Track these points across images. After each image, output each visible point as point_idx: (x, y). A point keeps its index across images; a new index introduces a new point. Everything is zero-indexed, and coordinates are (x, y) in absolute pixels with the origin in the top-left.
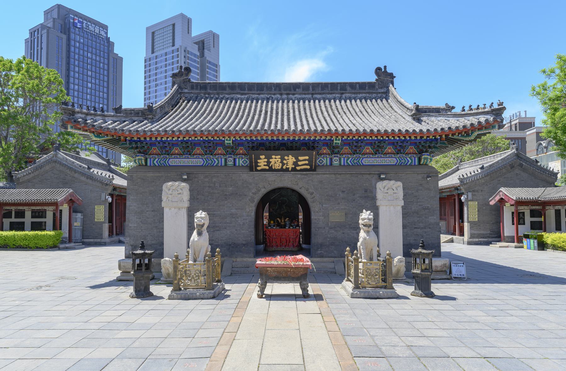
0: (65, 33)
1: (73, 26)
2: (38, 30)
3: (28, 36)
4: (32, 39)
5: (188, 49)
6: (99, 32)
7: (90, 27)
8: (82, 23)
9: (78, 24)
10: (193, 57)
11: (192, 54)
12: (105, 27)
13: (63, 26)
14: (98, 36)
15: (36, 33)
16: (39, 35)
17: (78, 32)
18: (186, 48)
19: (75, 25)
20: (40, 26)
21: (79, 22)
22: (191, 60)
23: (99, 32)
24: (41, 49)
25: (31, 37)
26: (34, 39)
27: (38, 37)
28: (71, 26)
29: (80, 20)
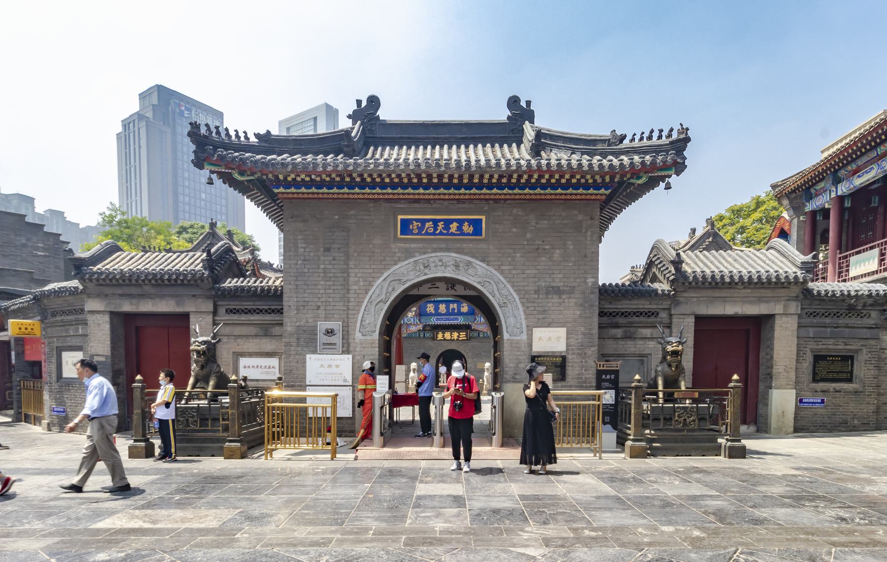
4: (127, 133)
7: (200, 115)
9: (186, 112)
15: (131, 125)
16: (136, 129)
20: (136, 117)
21: (187, 109)
24: (140, 147)
25: (125, 131)
26: (129, 134)
27: (134, 131)
29: (187, 106)
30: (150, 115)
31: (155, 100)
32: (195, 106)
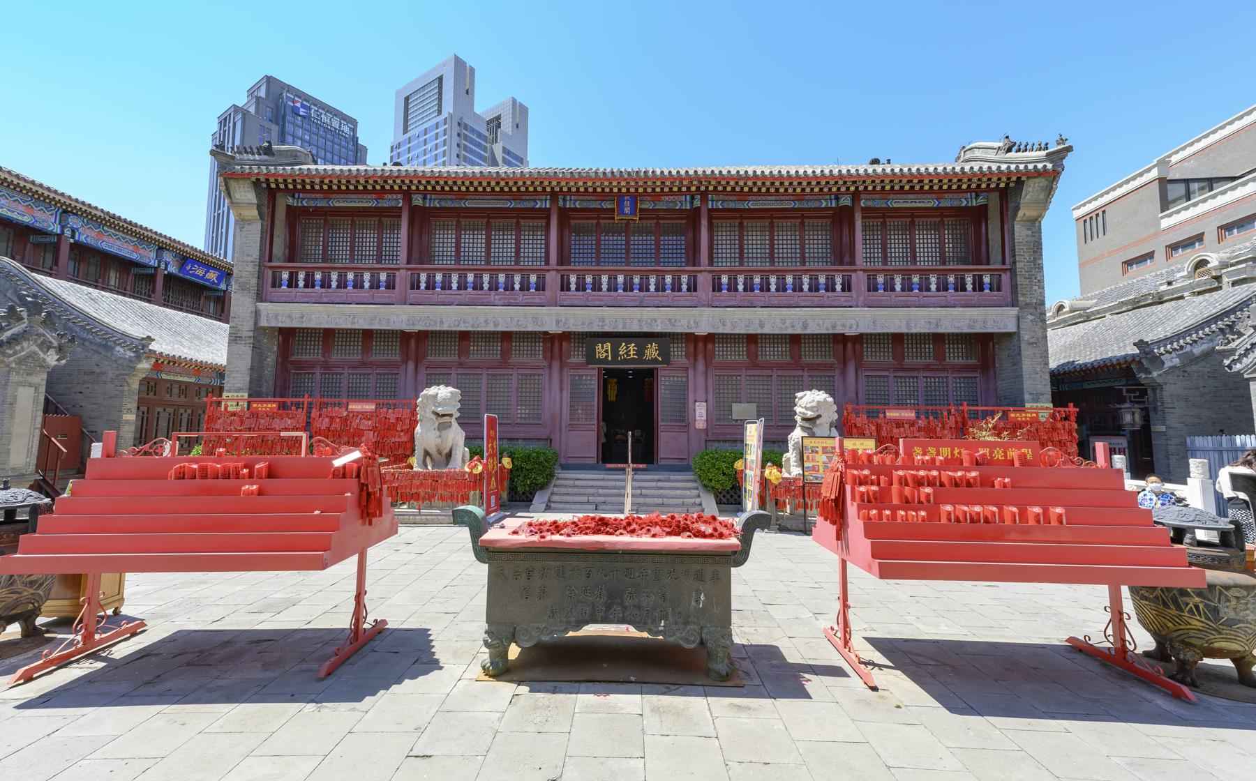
0: (277, 123)
1: (293, 112)
2: (230, 115)
3: (215, 128)
4: (222, 132)
5: (465, 120)
6: (340, 127)
8: (310, 109)
9: (301, 110)
10: (475, 137)
11: (473, 131)
12: (353, 123)
13: (275, 112)
14: (337, 133)
16: (231, 125)
17: (300, 123)
18: (461, 119)
19: (295, 112)
22: (471, 143)
23: (340, 127)
28: (289, 112)
29: (305, 103)
30: (252, 110)
31: (262, 93)
32: (315, 105)
